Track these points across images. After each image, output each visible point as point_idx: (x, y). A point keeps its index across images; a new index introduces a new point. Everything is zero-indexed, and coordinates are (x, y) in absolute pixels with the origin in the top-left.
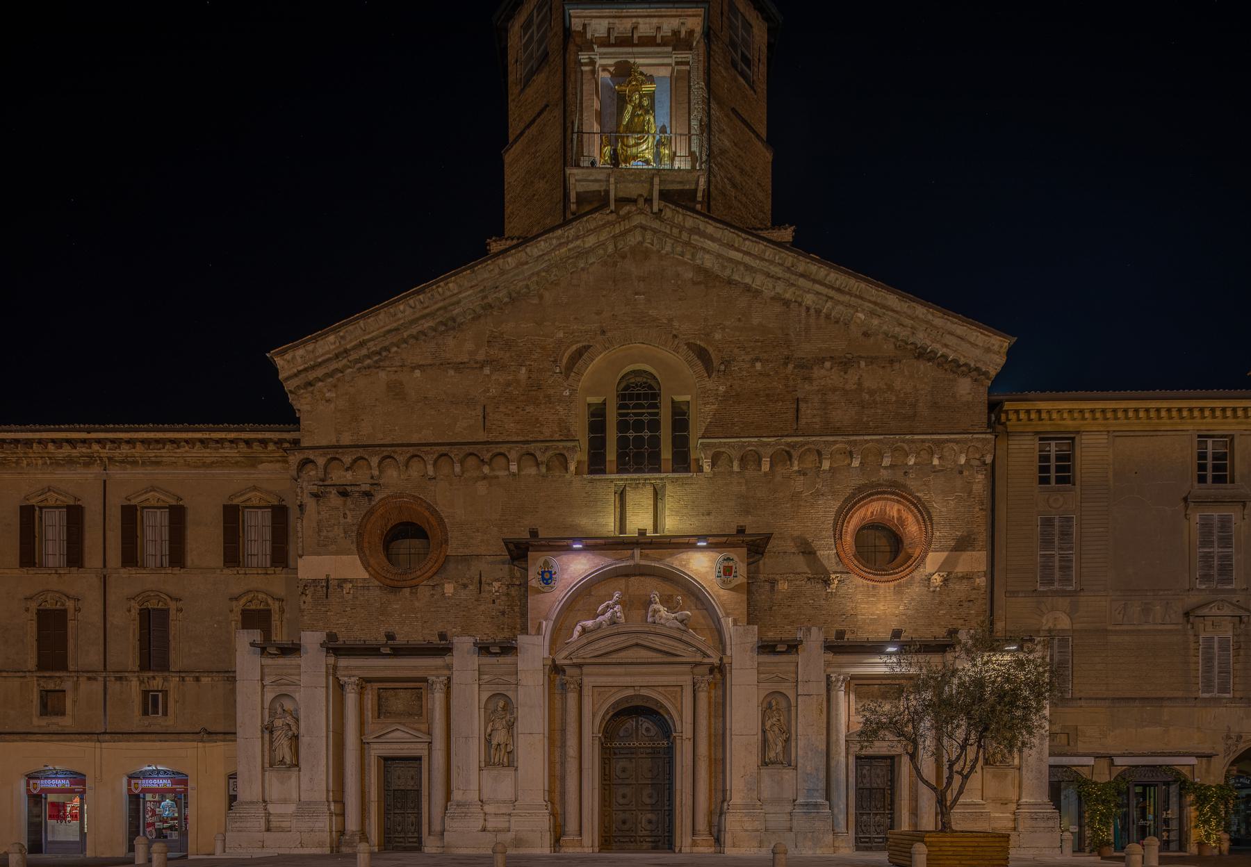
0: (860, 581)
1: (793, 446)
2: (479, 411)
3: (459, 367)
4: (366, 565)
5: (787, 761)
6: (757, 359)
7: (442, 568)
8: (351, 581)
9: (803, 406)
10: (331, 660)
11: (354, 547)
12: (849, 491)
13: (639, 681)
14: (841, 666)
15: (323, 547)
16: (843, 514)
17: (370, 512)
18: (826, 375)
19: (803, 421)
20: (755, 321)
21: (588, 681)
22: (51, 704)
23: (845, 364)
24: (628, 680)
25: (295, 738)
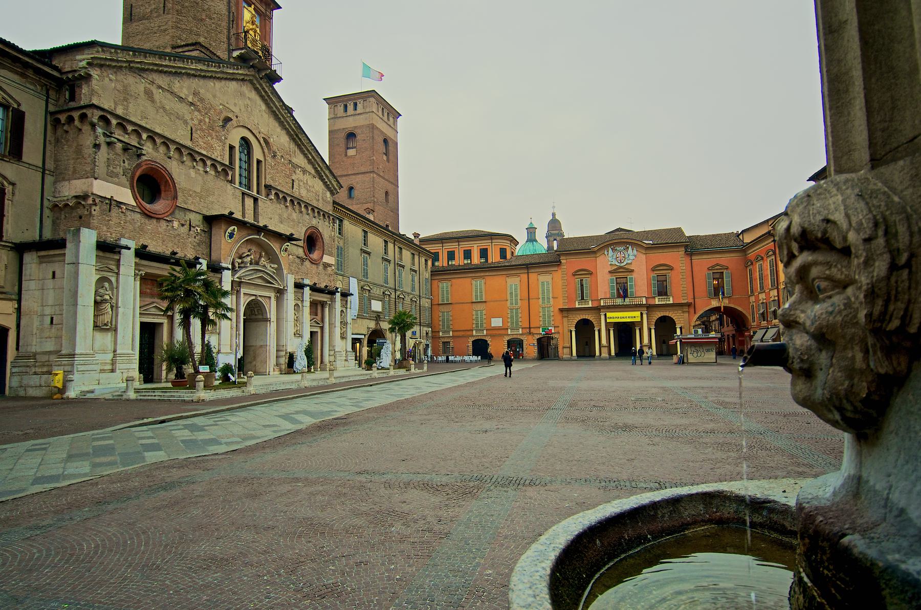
2: (189, 129)
3: (181, 99)
4: (135, 198)
5: (301, 336)
7: (173, 213)
8: (125, 204)
10: (138, 260)
11: (128, 184)
13: (258, 293)
15: (111, 176)
17: (139, 166)
20: (282, 141)
21: (243, 291)
23: (304, 171)
24: (254, 292)
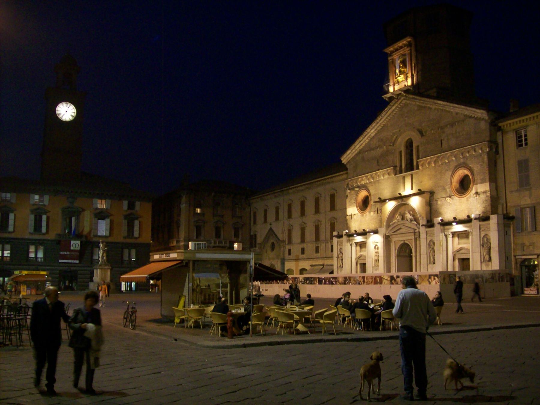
0: (457, 198)
1: (438, 157)
6: (432, 130)
9: (443, 142)
12: (453, 168)
14: (448, 229)
16: (452, 176)
18: (448, 130)
19: (443, 146)
21: (393, 240)
22: (317, 251)
23: (452, 125)
25: (342, 260)
